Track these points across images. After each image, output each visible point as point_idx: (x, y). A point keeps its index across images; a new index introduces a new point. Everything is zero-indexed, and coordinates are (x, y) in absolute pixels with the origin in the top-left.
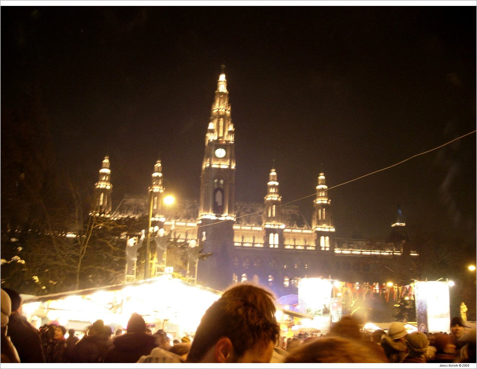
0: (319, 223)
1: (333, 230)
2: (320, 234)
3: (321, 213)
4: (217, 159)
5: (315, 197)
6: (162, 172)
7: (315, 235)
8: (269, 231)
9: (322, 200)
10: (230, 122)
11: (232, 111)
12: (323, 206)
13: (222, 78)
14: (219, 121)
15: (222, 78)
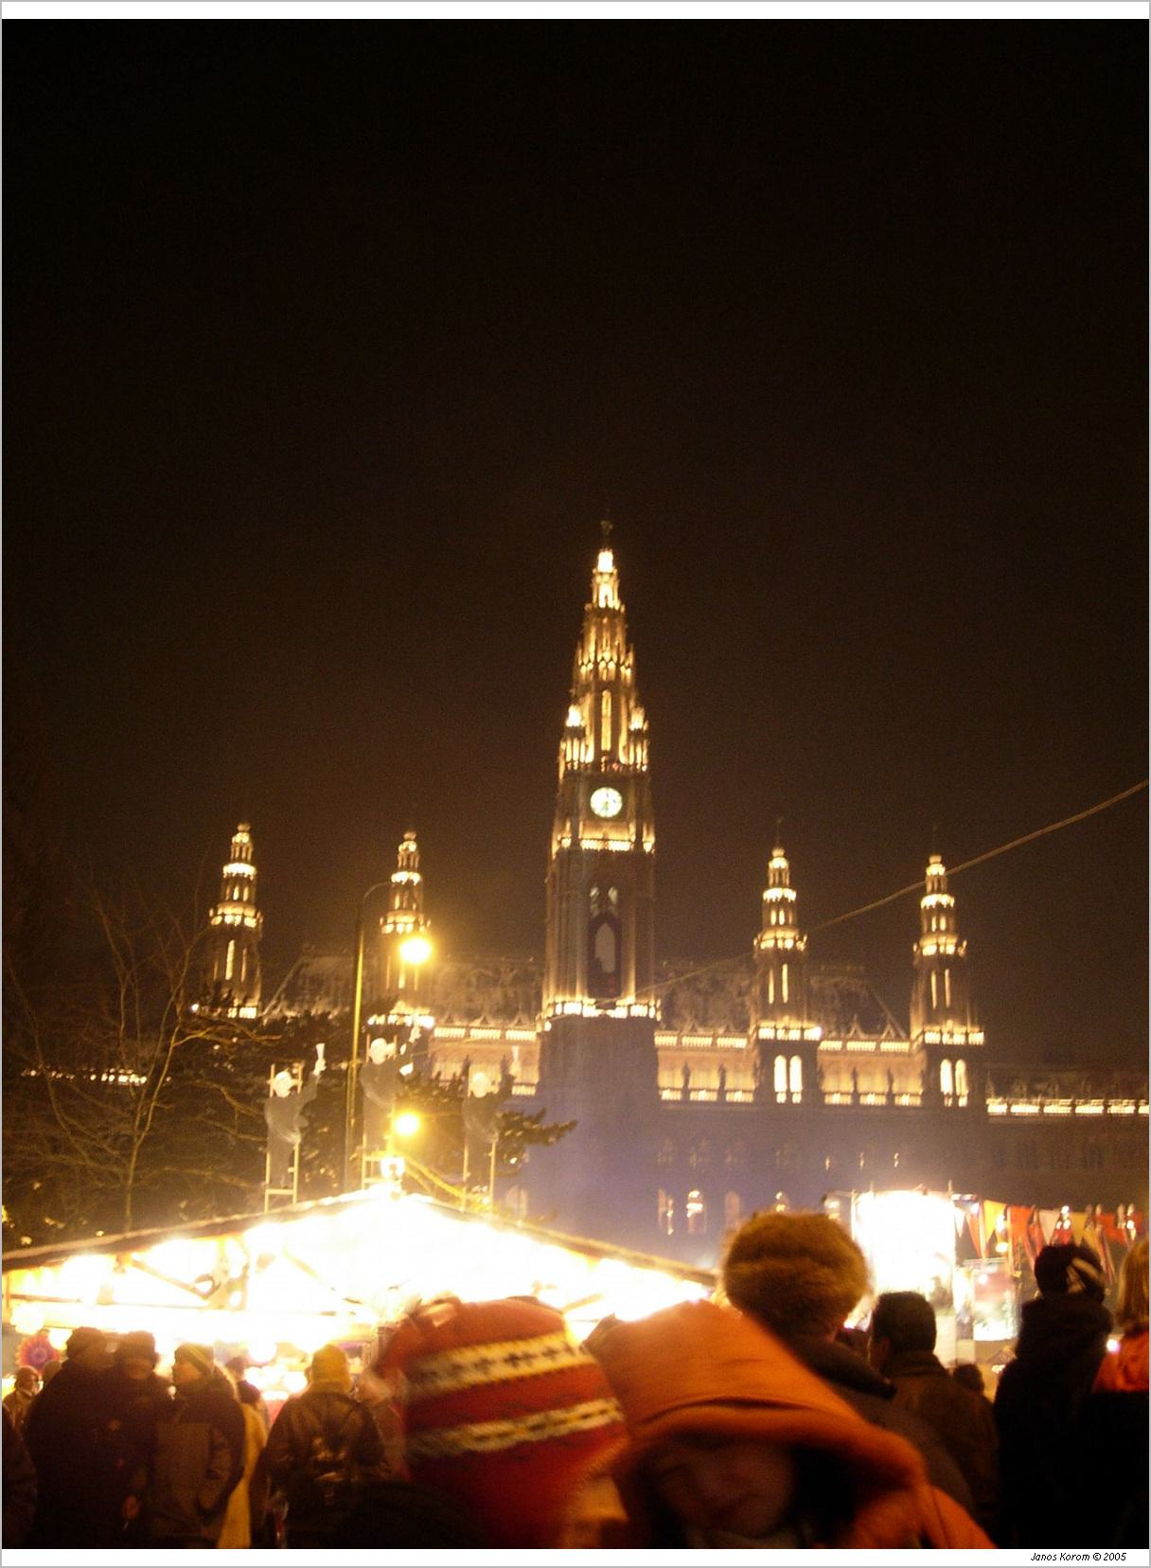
0: (932, 1018)
1: (978, 1038)
2: (936, 1054)
3: (940, 987)
4: (596, 821)
5: (917, 934)
6: (420, 871)
7: (920, 1058)
8: (769, 1050)
9: (938, 943)
10: (632, 704)
11: (638, 668)
12: (941, 961)
13: (606, 561)
14: (598, 701)
15: (606, 561)
